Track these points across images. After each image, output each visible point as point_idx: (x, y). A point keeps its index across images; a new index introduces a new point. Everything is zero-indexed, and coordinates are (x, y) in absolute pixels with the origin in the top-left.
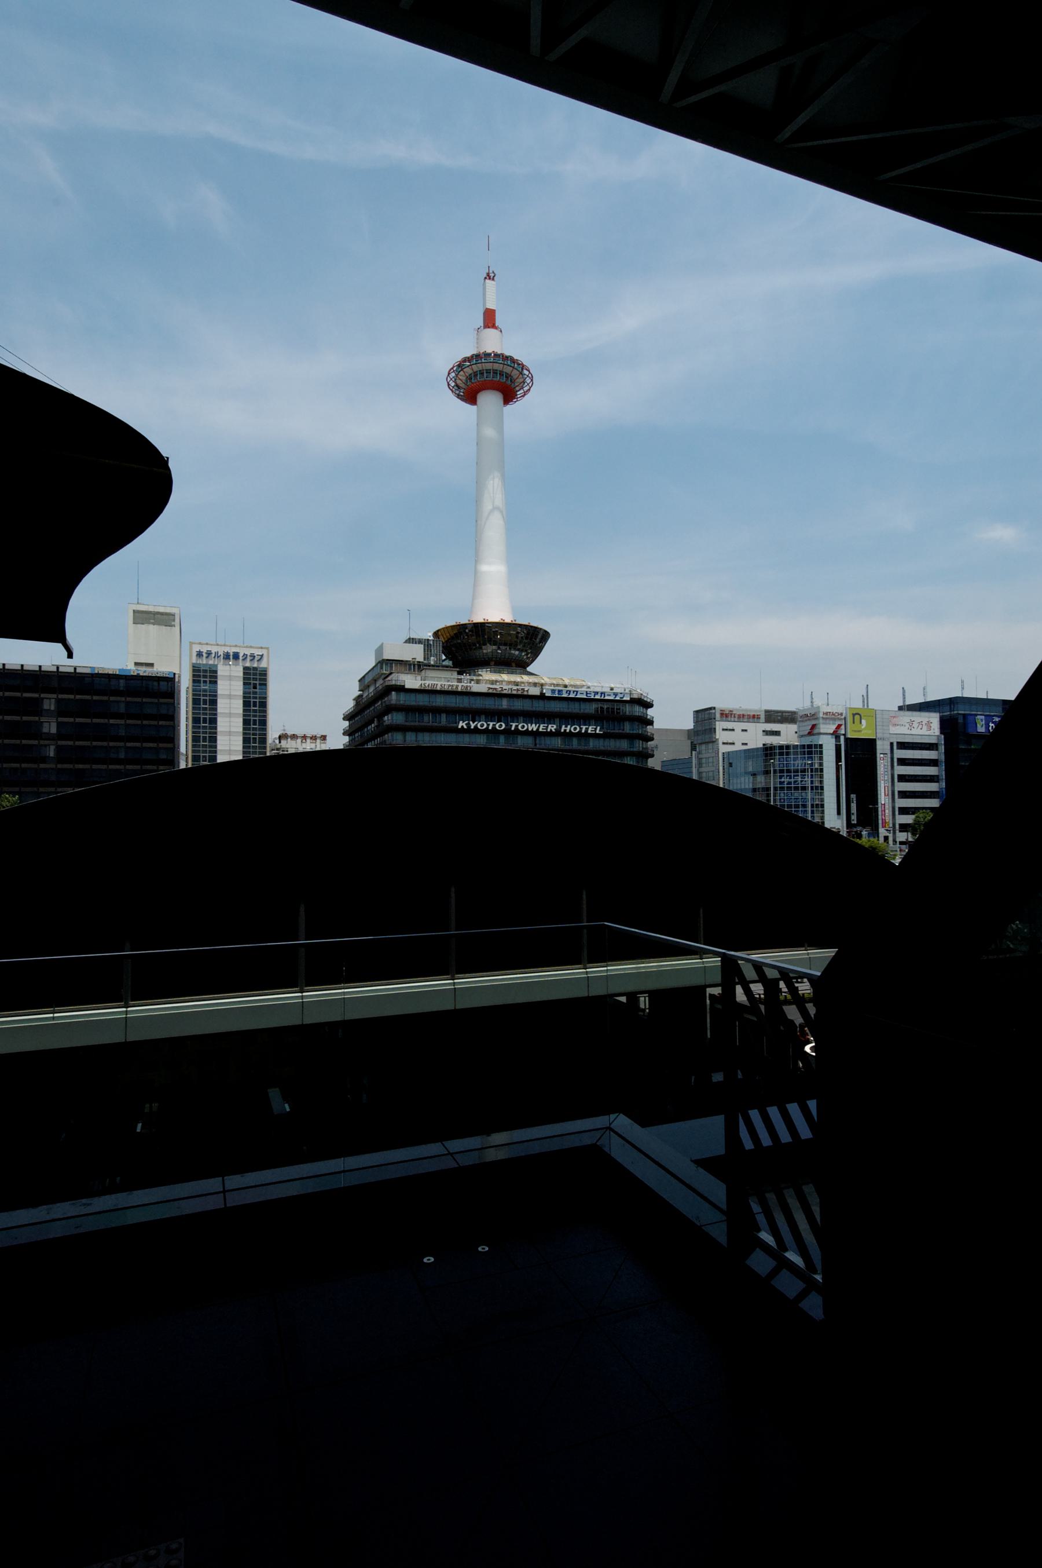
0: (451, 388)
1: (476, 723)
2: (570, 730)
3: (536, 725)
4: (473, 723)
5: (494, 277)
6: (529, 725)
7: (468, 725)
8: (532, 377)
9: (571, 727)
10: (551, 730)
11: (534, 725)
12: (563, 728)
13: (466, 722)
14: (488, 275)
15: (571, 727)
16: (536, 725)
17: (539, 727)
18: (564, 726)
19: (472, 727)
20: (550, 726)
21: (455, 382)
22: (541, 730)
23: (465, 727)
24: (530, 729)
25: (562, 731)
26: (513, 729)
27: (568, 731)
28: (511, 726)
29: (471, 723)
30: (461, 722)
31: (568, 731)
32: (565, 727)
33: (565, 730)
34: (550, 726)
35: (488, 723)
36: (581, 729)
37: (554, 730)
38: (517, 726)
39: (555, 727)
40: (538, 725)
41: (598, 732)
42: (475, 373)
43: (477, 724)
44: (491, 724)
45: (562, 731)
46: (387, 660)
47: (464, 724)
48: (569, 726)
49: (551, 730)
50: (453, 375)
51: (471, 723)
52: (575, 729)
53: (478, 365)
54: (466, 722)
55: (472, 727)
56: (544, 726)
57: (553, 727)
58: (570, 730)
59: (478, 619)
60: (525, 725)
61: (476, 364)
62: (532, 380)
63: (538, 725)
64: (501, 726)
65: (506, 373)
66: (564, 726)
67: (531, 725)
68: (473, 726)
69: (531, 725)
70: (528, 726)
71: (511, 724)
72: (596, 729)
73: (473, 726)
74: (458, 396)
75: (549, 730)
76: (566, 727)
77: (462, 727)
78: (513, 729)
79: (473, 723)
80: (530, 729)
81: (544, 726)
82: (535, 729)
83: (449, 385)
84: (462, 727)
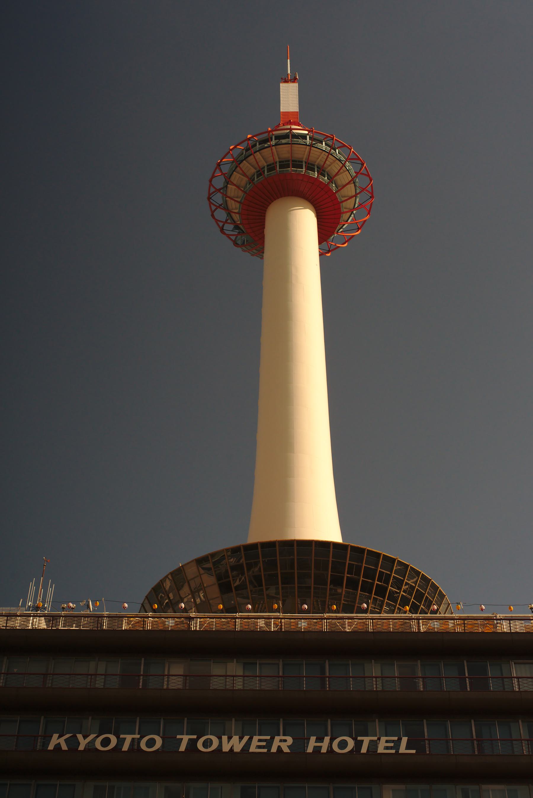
2: (330, 750)
3: (241, 738)
4: (85, 737)
6: (225, 738)
7: (73, 742)
9: (332, 740)
10: (279, 748)
11: (236, 738)
12: (312, 743)
13: (68, 736)
15: (332, 740)
16: (241, 738)
19: (81, 748)
20: (277, 739)
23: (64, 747)
24: (226, 748)
25: (310, 750)
26: (182, 748)
27: (324, 750)
29: (80, 737)
30: (55, 736)
31: (324, 750)
33: (317, 750)
37: (286, 750)
38: (192, 743)
39: (290, 740)
40: (246, 738)
43: (94, 740)
44: (129, 738)
45: (310, 750)
47: (62, 741)
48: (327, 739)
49: (279, 748)
51: (80, 737)
54: (68, 736)
55: (81, 748)
56: (260, 740)
57: (285, 741)
58: (330, 750)
63: (246, 738)
64: (151, 743)
66: (313, 739)
68: (83, 743)
69: (230, 738)
71: (179, 737)
73: (83, 743)
75: (274, 749)
76: (320, 739)
77: (58, 747)
78: (182, 748)
79: (85, 737)
80: (226, 748)
82: (238, 748)
84: (58, 747)
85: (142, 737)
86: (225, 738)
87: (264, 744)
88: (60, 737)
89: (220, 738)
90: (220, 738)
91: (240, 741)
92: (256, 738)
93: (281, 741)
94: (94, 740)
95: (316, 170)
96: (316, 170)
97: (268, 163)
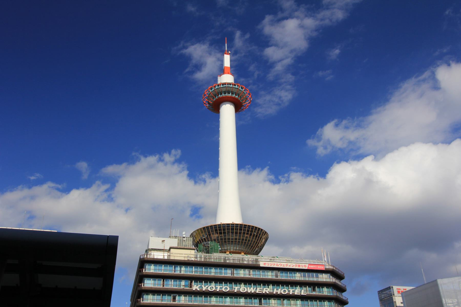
1: (207, 286)
3: (254, 289)
4: (205, 286)
6: (248, 288)
10: (266, 292)
11: (252, 288)
16: (254, 289)
17: (257, 289)
18: (275, 289)
20: (265, 289)
22: (257, 292)
28: (235, 288)
29: (203, 286)
32: (277, 290)
34: (265, 289)
35: (216, 286)
36: (289, 291)
37: (268, 293)
40: (255, 288)
41: (302, 294)
43: (207, 288)
46: (152, 249)
48: (279, 290)
49: (266, 292)
52: (285, 291)
53: (219, 89)
56: (259, 289)
57: (267, 290)
59: (218, 223)
60: (246, 288)
61: (217, 89)
64: (227, 288)
65: (235, 92)
66: (275, 289)
67: (250, 288)
69: (250, 288)
70: (247, 289)
72: (301, 291)
79: (205, 286)
80: (249, 292)
81: (259, 289)
85: (223, 287)
86: (248, 288)
87: (261, 290)
88: (197, 286)
89: (247, 288)
90: (247, 288)
91: (253, 290)
92: (258, 289)
93: (266, 290)
94: (207, 288)
95: (231, 93)
96: (231, 93)
97: (224, 91)
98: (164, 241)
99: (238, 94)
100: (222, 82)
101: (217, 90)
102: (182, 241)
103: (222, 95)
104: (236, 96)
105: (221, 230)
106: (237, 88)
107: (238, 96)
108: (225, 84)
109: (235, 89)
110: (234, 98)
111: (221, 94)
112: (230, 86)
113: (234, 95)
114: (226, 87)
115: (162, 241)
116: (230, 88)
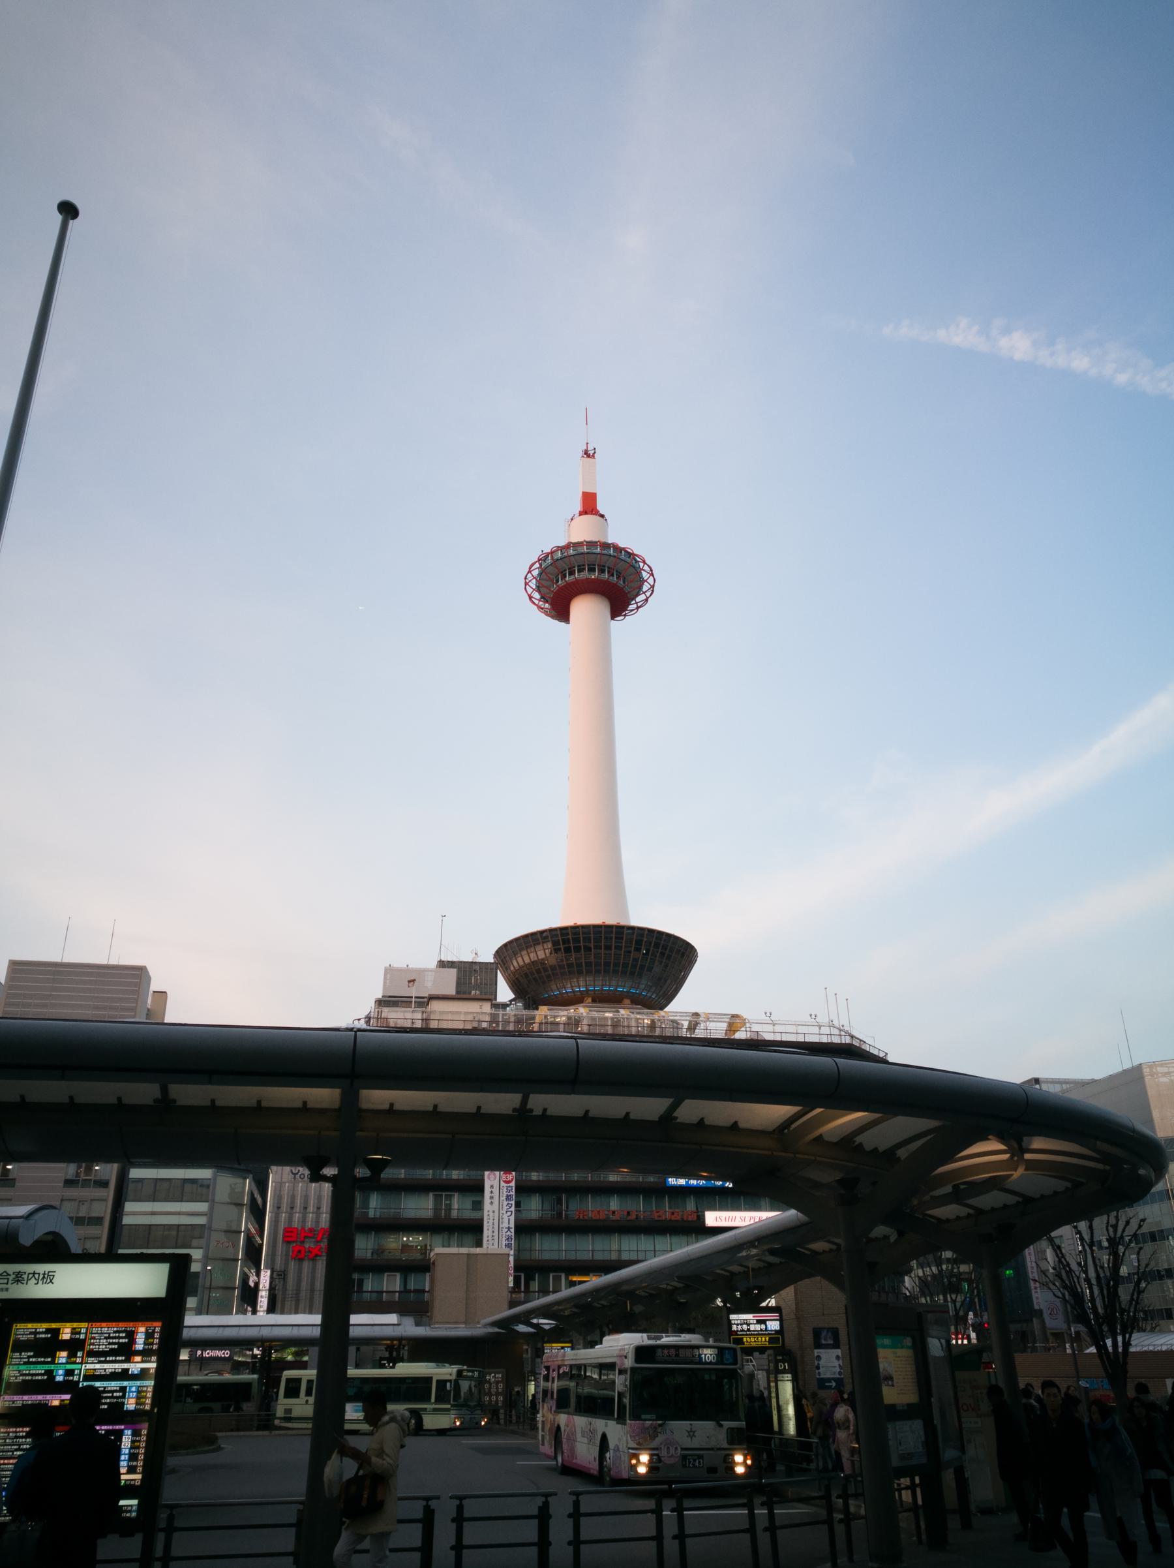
0: (537, 602)
5: (595, 453)
8: (651, 570)
14: (586, 453)
21: (539, 592)
42: (562, 572)
50: (533, 584)
53: (565, 560)
61: (561, 559)
62: (652, 575)
74: (546, 614)
83: (530, 597)
98: (413, 981)
99: (617, 571)
100: (573, 541)
101: (559, 564)
102: (470, 972)
103: (573, 577)
104: (611, 578)
105: (569, 942)
106: (615, 556)
107: (617, 578)
108: (579, 544)
109: (608, 557)
110: (607, 582)
111: (572, 573)
112: (595, 551)
113: (607, 577)
114: (582, 553)
115: (409, 982)
116: (595, 555)
